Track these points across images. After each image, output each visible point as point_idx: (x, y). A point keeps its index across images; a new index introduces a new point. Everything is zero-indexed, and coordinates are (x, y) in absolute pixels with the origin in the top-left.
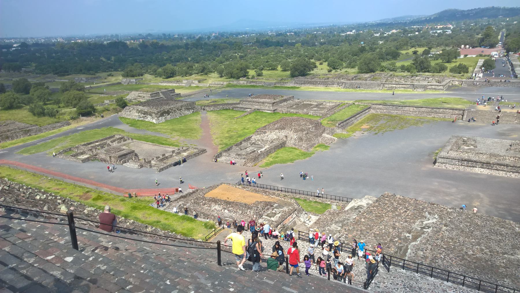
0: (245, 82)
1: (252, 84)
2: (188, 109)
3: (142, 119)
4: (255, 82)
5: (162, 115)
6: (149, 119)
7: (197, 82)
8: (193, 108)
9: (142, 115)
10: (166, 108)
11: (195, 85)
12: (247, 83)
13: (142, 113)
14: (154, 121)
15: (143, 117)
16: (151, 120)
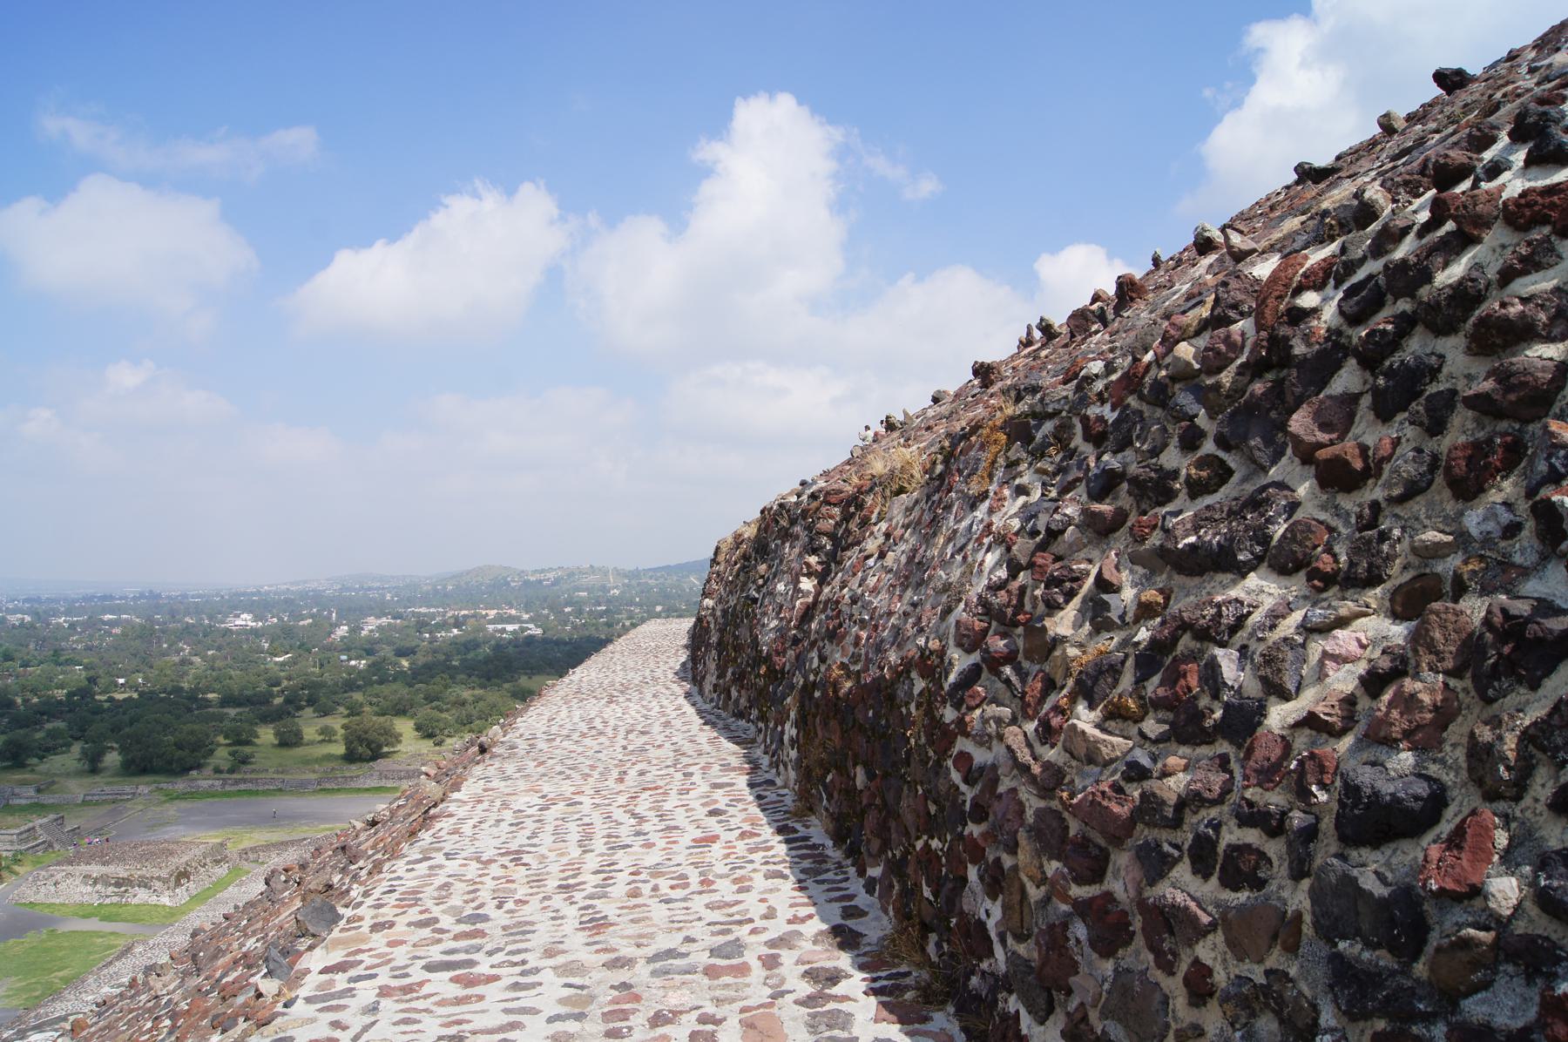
0: (217, 783)
1: (242, 787)
2: (217, 862)
3: (115, 899)
4: (251, 781)
5: (178, 884)
6: (142, 896)
7: (32, 792)
8: (224, 859)
9: (111, 889)
10: (179, 861)
11: (24, 802)
12: (223, 785)
13: (108, 884)
14: (165, 900)
15: (116, 894)
16: (153, 900)
